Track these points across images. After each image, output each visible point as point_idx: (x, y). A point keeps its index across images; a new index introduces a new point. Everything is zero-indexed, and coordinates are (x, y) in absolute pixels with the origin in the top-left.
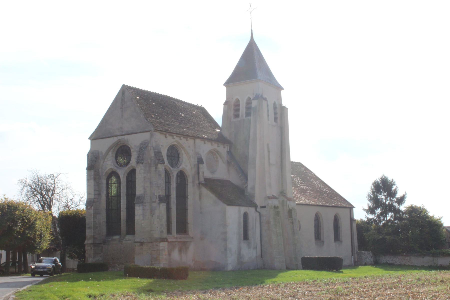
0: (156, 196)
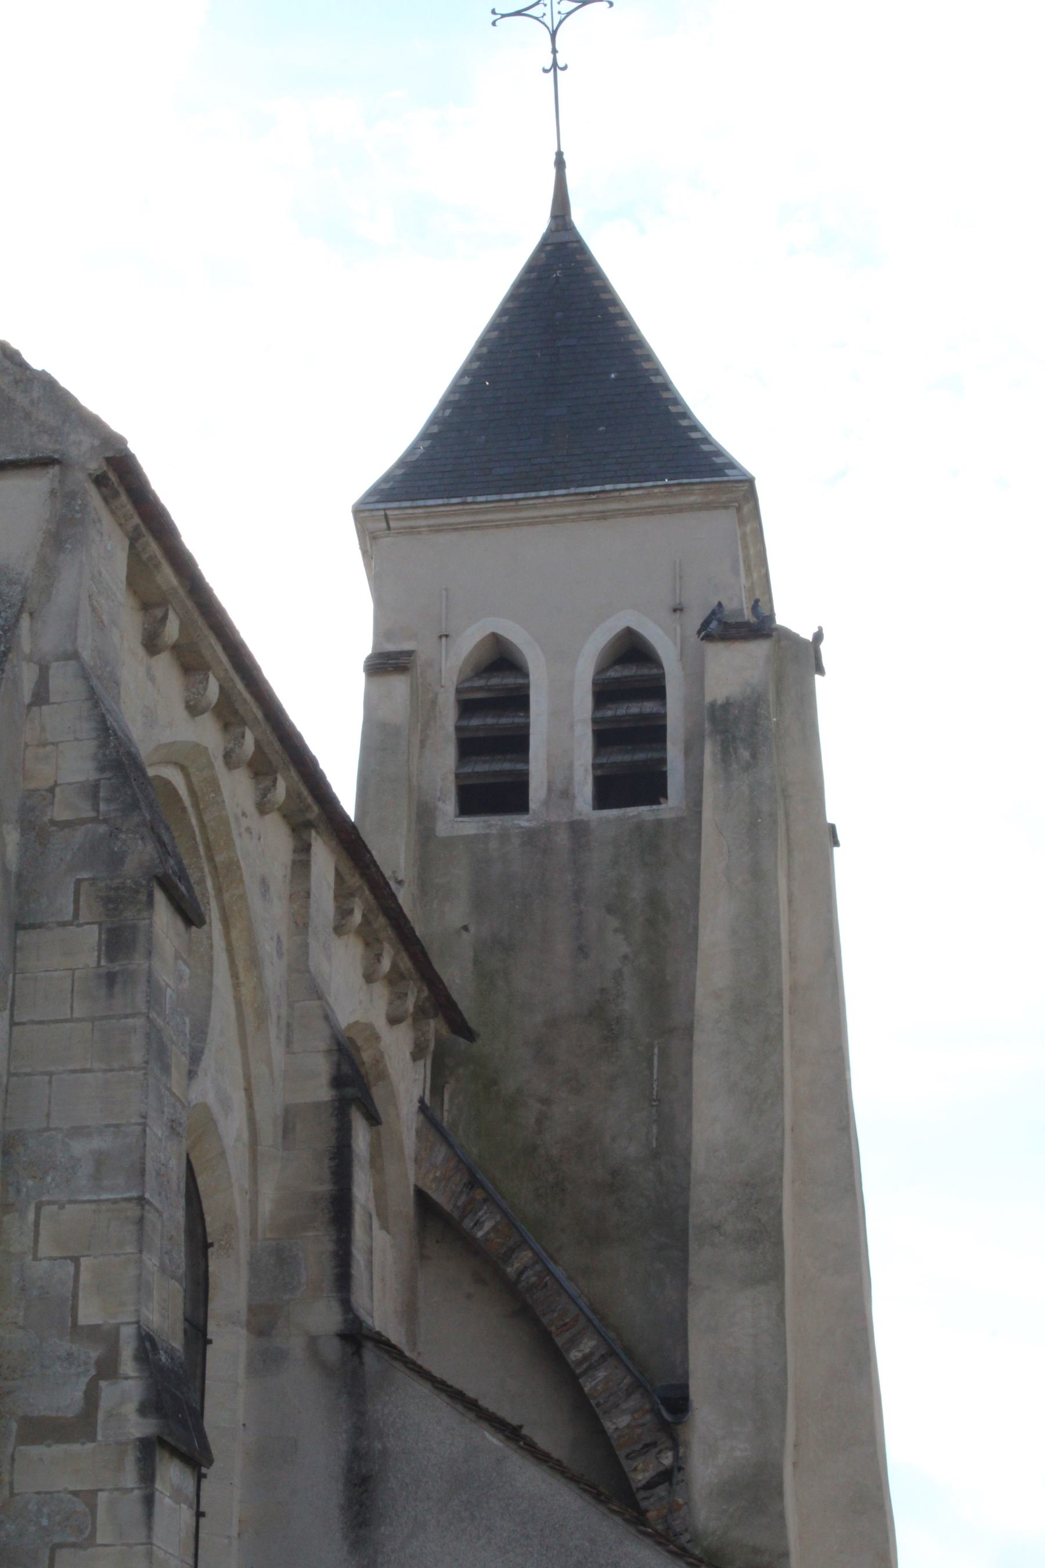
0: (107, 1338)
